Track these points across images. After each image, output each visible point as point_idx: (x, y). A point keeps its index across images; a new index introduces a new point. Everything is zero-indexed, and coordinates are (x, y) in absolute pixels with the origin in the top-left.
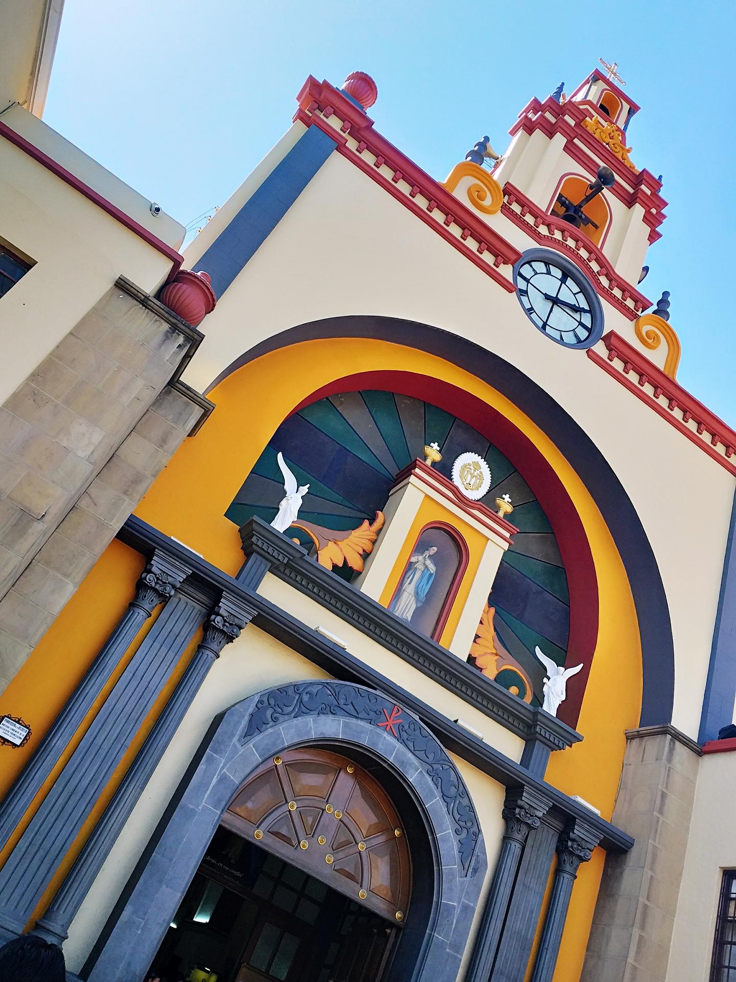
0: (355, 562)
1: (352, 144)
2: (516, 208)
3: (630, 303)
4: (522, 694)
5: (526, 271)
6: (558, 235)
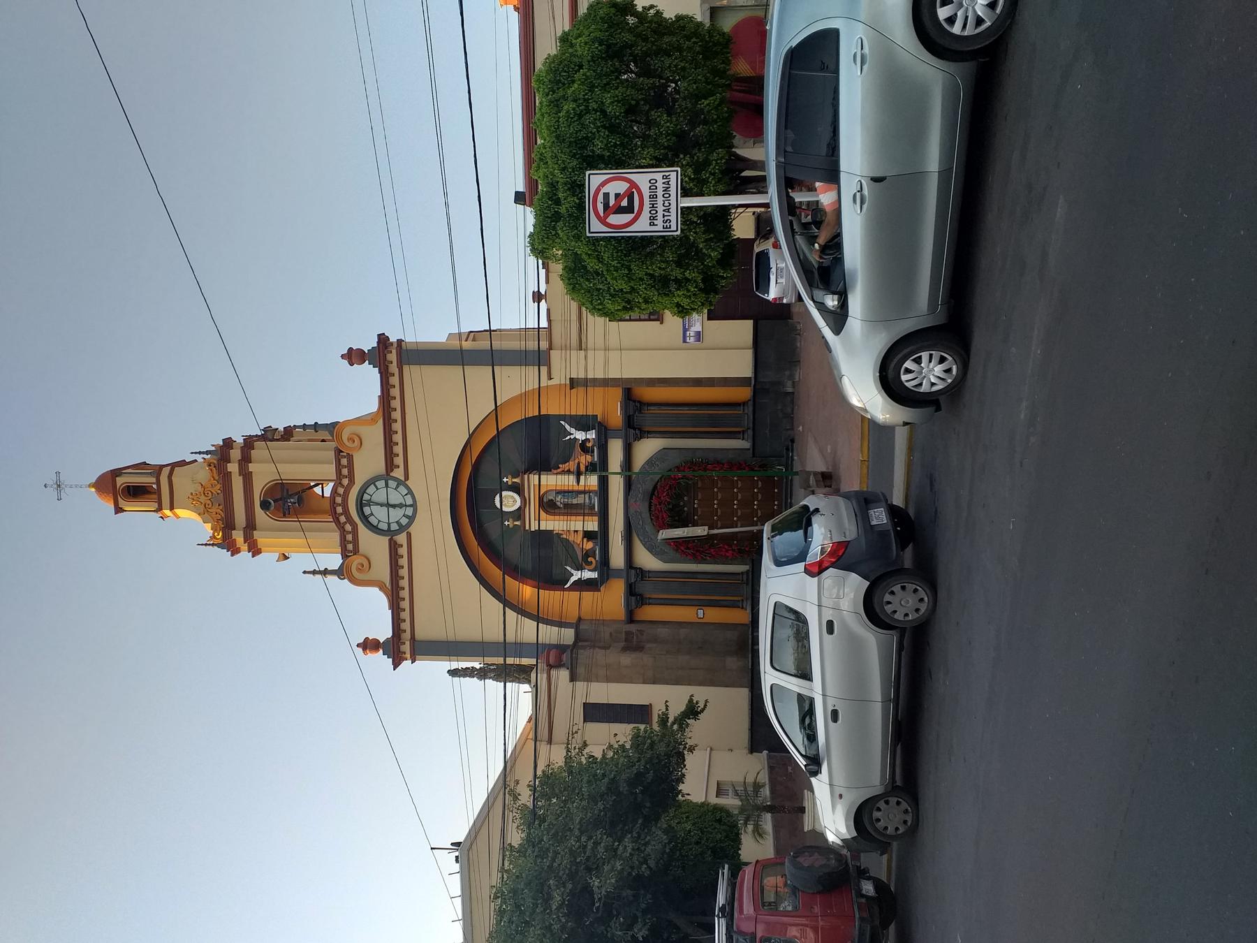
0: (581, 535)
1: (407, 635)
2: (350, 547)
3: (344, 461)
4: (587, 440)
5: (384, 526)
6: (343, 519)
